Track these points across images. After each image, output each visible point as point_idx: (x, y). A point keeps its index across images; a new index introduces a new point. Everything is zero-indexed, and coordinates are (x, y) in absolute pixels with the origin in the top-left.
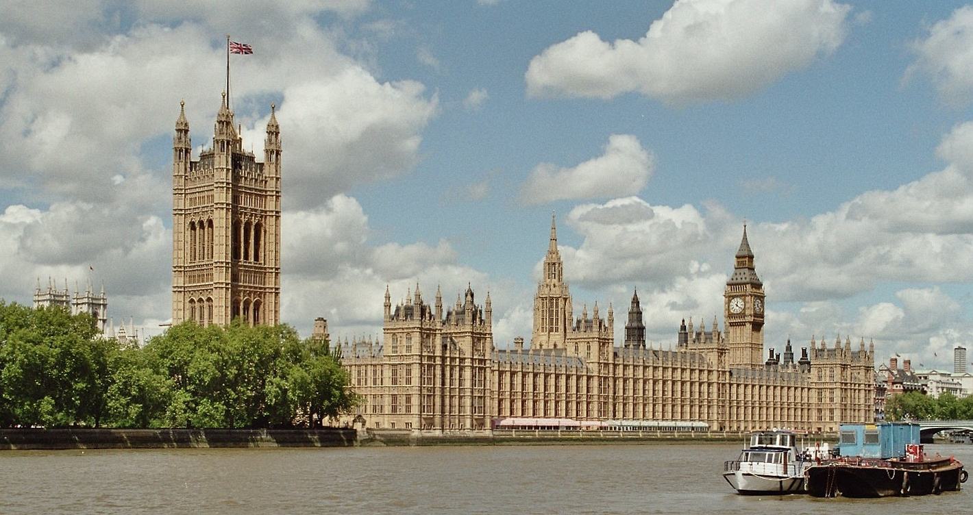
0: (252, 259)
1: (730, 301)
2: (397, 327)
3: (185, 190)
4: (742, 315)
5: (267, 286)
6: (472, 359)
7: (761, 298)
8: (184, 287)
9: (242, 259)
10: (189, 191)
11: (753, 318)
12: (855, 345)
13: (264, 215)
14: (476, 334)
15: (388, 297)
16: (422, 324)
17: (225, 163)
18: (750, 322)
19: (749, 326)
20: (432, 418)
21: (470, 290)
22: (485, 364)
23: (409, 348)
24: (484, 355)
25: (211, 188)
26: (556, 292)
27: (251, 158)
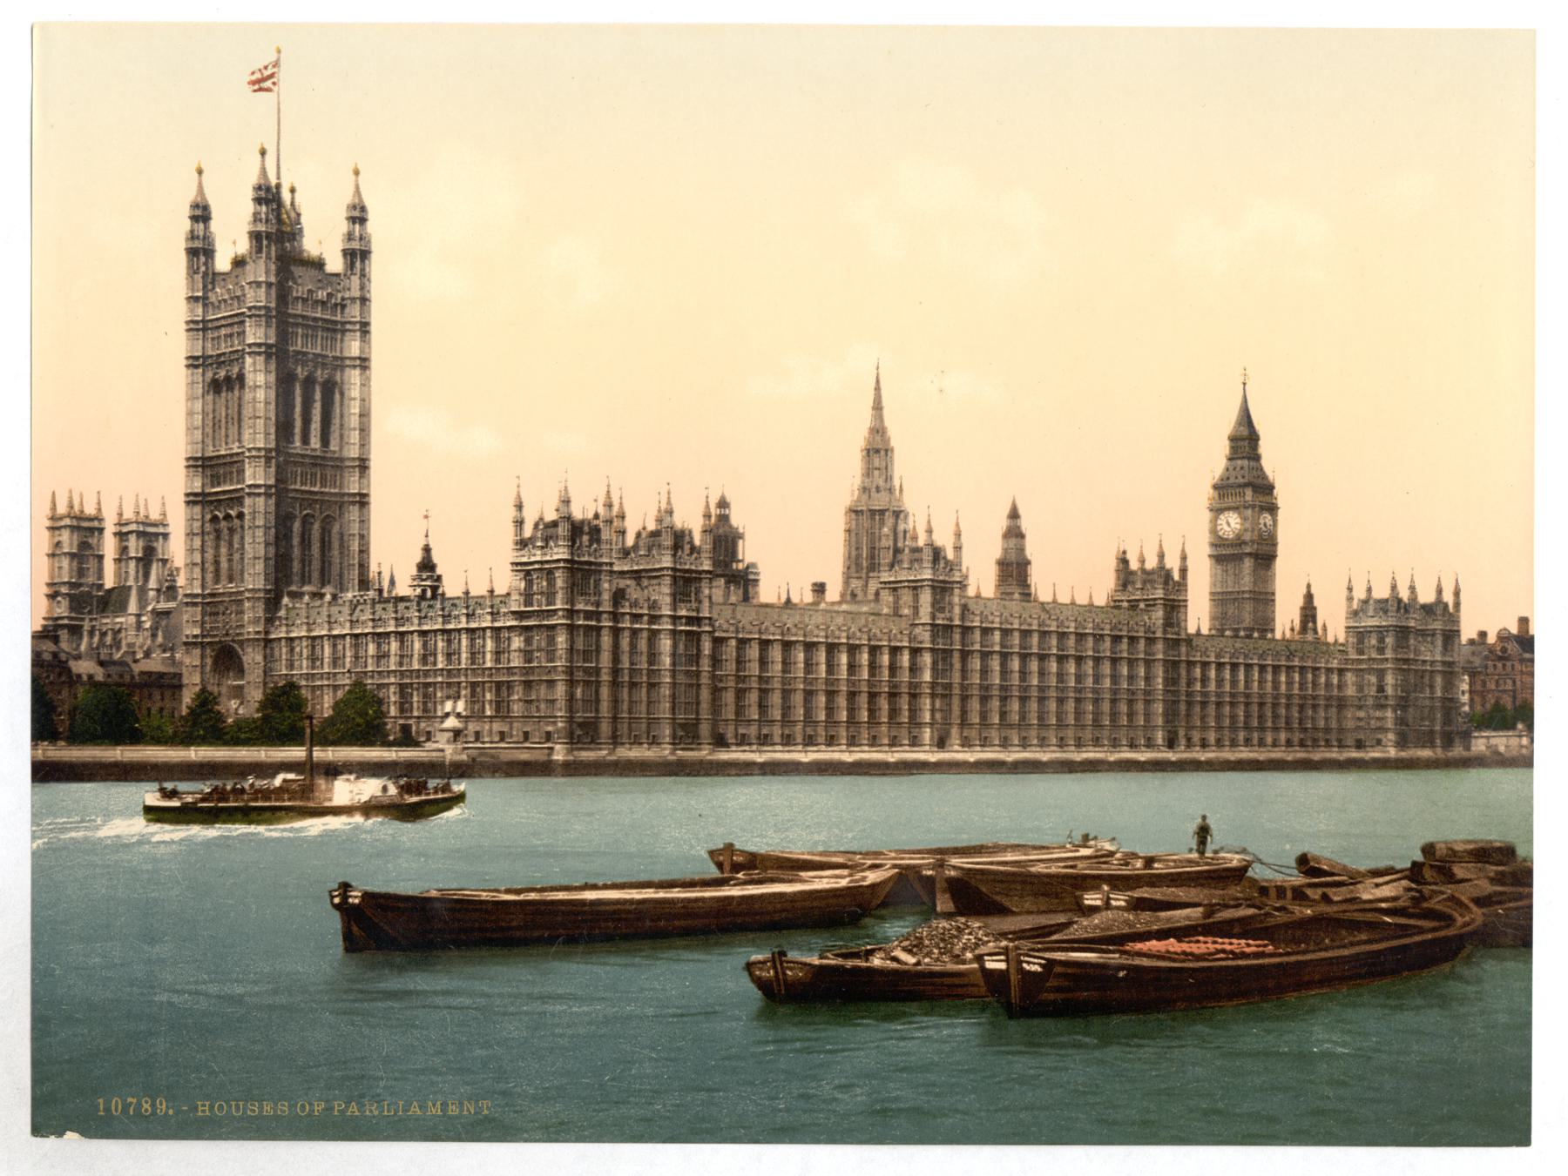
0: (315, 442)
1: (1216, 518)
2: (533, 559)
4: (1239, 542)
5: (347, 491)
7: (1272, 509)
9: (298, 444)
10: (210, 325)
11: (1256, 546)
12: (1426, 596)
13: (340, 363)
14: (680, 570)
16: (572, 554)
18: (1250, 554)
20: (693, 724)
24: (698, 610)
26: (880, 501)
27: (319, 264)
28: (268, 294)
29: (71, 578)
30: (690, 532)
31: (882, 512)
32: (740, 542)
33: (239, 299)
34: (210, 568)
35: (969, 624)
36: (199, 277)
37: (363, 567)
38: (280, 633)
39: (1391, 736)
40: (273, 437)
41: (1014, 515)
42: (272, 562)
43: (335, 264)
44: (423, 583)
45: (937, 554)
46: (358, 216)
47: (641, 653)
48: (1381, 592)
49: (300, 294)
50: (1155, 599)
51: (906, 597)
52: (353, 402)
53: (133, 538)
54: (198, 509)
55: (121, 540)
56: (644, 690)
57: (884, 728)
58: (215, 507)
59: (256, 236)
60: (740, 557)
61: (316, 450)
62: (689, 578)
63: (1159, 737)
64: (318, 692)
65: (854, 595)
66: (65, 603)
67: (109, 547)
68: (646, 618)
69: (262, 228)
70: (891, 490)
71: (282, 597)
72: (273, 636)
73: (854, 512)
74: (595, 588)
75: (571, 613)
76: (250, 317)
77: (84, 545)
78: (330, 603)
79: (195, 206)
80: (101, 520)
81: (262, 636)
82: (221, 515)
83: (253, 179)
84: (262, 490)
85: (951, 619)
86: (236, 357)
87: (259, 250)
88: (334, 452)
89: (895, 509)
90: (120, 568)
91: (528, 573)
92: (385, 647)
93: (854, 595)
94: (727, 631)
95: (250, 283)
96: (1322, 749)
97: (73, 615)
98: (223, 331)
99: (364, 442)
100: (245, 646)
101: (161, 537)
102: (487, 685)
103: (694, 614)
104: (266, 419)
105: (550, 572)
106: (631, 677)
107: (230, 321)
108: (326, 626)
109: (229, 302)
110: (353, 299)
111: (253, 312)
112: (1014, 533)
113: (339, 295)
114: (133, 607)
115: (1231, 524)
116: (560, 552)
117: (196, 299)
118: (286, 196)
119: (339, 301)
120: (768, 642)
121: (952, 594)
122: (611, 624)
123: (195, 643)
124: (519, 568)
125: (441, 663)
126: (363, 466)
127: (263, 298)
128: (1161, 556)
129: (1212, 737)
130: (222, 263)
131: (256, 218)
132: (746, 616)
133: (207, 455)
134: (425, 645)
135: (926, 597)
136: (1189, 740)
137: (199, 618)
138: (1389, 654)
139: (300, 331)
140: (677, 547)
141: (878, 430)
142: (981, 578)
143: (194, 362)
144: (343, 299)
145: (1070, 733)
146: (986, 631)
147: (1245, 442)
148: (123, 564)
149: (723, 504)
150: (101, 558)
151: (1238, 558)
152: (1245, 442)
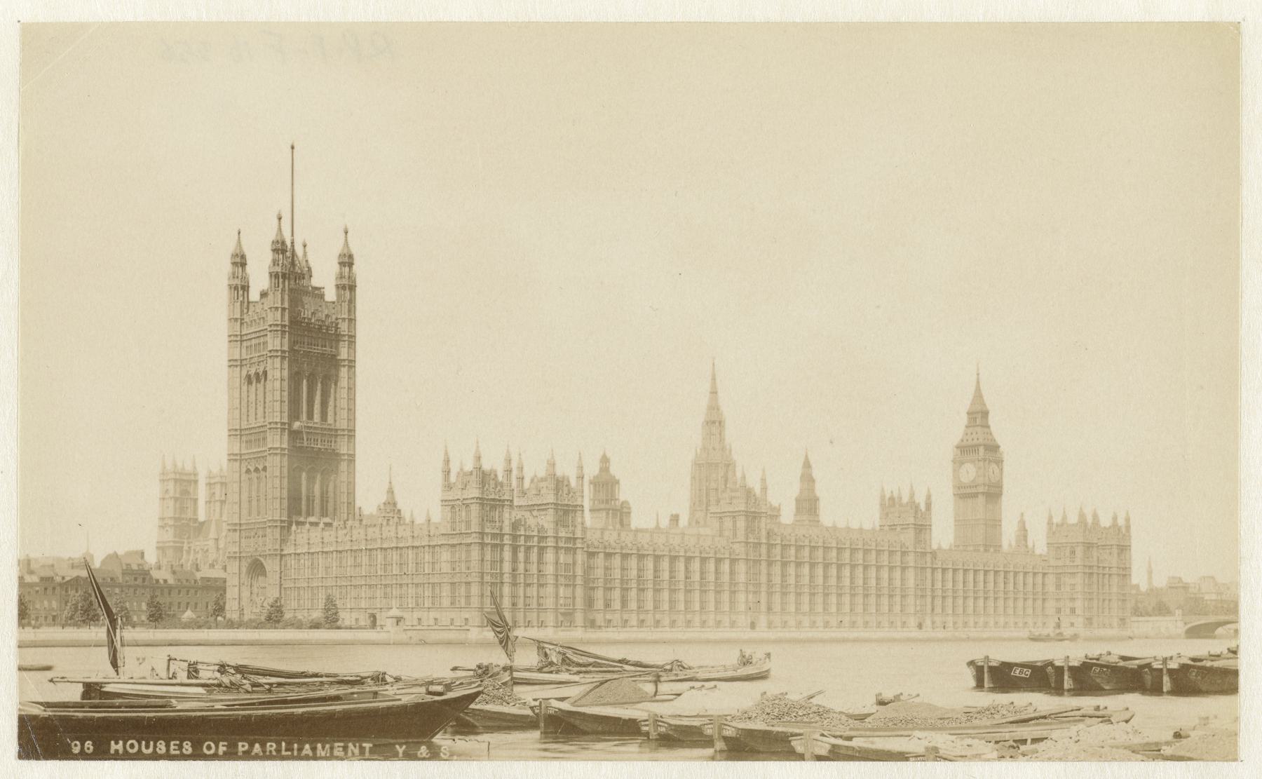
0: (317, 416)
3: (241, 335)
6: (557, 538)
7: (999, 462)
8: (241, 455)
10: (245, 338)
15: (447, 461)
16: (483, 493)
17: (280, 303)
19: (981, 499)
22: (575, 544)
23: (468, 523)
25: (265, 333)
28: (282, 315)
29: (175, 514)
30: (496, 471)
32: (617, 486)
34: (245, 505)
35: (773, 542)
37: (351, 504)
38: (289, 550)
39: (1081, 620)
40: (286, 414)
41: (807, 465)
42: (285, 503)
43: (330, 295)
44: (387, 515)
46: (347, 261)
47: (533, 563)
49: (306, 316)
50: (908, 524)
51: (728, 523)
52: (342, 390)
53: (218, 486)
55: (210, 489)
56: (535, 588)
57: (712, 616)
58: (249, 463)
59: (274, 276)
60: (617, 497)
61: (317, 423)
62: (568, 511)
63: (912, 622)
64: (288, 592)
65: (697, 522)
66: (171, 531)
67: (202, 493)
68: (536, 539)
69: (278, 269)
70: (723, 449)
71: (292, 525)
72: (285, 552)
73: (697, 465)
74: (499, 517)
75: (482, 534)
76: (271, 331)
77: (185, 492)
78: (323, 529)
79: (235, 256)
80: (195, 475)
81: (279, 552)
82: (252, 469)
83: (272, 236)
84: (279, 451)
85: (759, 538)
86: (262, 359)
88: (330, 425)
89: (726, 462)
90: (210, 507)
91: (453, 507)
92: (359, 560)
93: (697, 522)
94: (598, 548)
95: (270, 308)
96: (635, 629)
97: (177, 539)
98: (253, 342)
100: (268, 558)
101: (193, 483)
102: (426, 585)
103: (571, 535)
104: (281, 402)
105: (467, 506)
106: (538, 580)
107: (258, 335)
108: (307, 546)
109: (258, 321)
110: (344, 319)
111: (273, 328)
112: (808, 479)
113: (334, 317)
114: (212, 535)
115: (969, 472)
116: (473, 492)
117: (236, 320)
118: (299, 251)
119: (333, 320)
120: (644, 556)
121: (759, 522)
122: (511, 543)
123: (235, 557)
124: (447, 503)
125: (396, 570)
126: (351, 434)
127: (279, 318)
128: (912, 495)
129: (834, 621)
130: (254, 295)
131: (275, 262)
132: (627, 538)
133: (243, 427)
134: (385, 558)
135: (741, 523)
136: (933, 623)
138: (1078, 562)
139: (306, 341)
140: (557, 489)
141: (714, 407)
143: (232, 363)
144: (337, 319)
145: (650, 619)
146: (785, 547)
147: (979, 416)
148: (212, 504)
150: (196, 500)
151: (975, 495)
152: (979, 416)
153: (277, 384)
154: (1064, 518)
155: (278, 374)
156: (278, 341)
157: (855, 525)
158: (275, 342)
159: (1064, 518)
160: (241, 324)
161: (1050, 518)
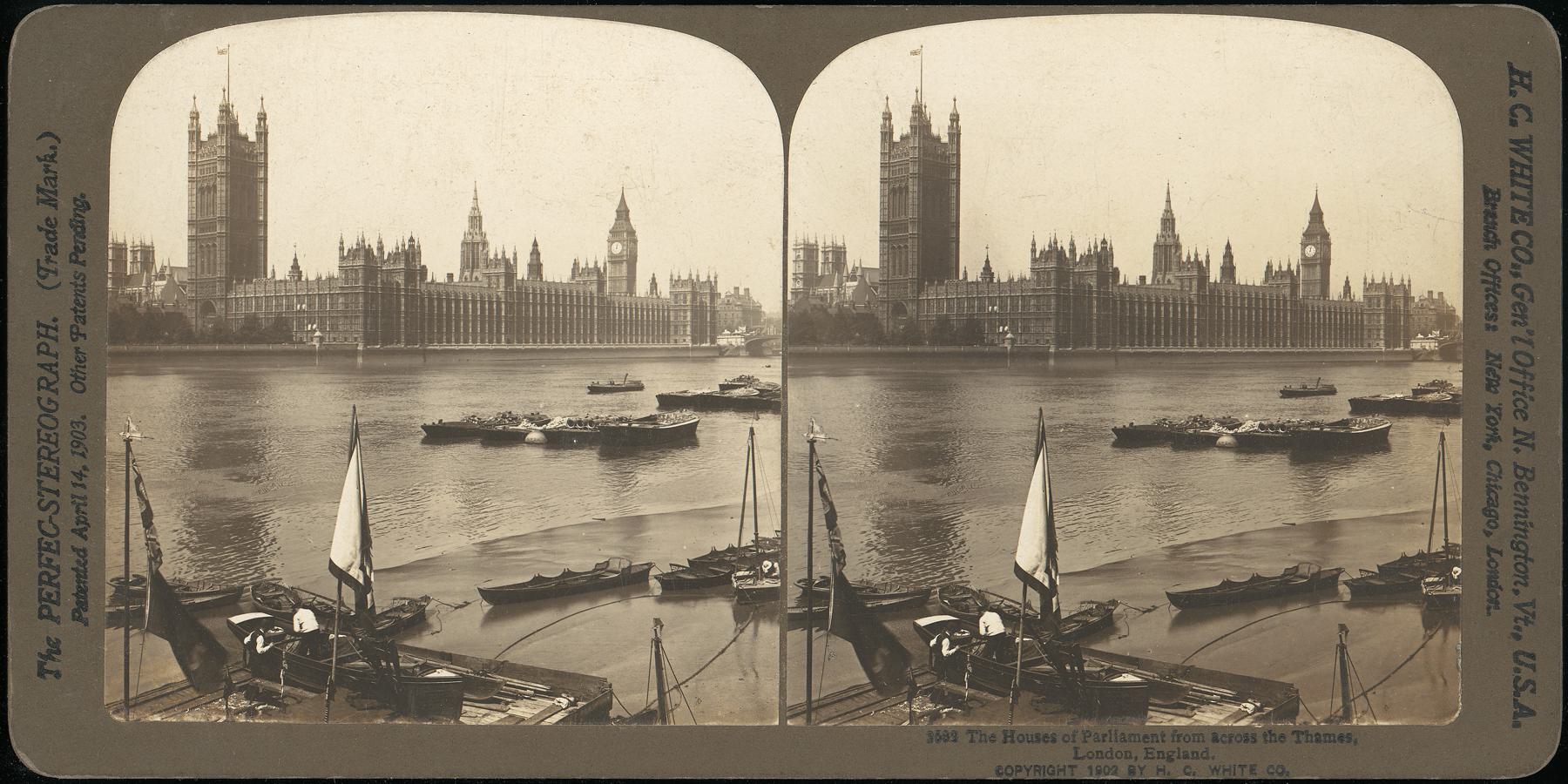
21: (412, 237)
26: (478, 238)
27: (245, 138)
28: (227, 152)
31: (478, 243)
33: (215, 153)
34: (199, 267)
36: (194, 144)
39: (690, 338)
41: (535, 244)
45: (507, 261)
46: (262, 118)
48: (685, 277)
54: (194, 243)
73: (464, 244)
87: (223, 132)
99: (265, 215)
110: (261, 154)
117: (194, 153)
130: (204, 137)
135: (502, 280)
137: (194, 289)
142: (522, 272)
143: (191, 180)
149: (412, 240)
151: (621, 262)
153: (224, 194)
154: (679, 277)
155: (224, 188)
156: (224, 167)
157: (557, 281)
158: (220, 168)
159: (679, 277)
160: (197, 156)
161: (672, 276)
